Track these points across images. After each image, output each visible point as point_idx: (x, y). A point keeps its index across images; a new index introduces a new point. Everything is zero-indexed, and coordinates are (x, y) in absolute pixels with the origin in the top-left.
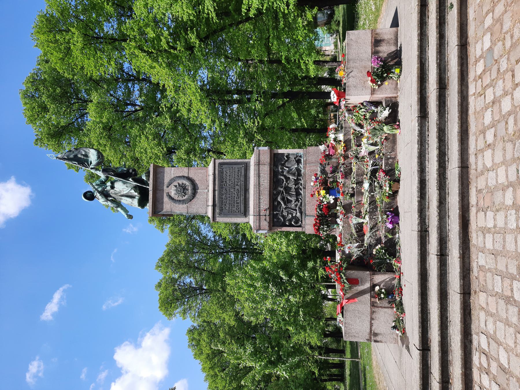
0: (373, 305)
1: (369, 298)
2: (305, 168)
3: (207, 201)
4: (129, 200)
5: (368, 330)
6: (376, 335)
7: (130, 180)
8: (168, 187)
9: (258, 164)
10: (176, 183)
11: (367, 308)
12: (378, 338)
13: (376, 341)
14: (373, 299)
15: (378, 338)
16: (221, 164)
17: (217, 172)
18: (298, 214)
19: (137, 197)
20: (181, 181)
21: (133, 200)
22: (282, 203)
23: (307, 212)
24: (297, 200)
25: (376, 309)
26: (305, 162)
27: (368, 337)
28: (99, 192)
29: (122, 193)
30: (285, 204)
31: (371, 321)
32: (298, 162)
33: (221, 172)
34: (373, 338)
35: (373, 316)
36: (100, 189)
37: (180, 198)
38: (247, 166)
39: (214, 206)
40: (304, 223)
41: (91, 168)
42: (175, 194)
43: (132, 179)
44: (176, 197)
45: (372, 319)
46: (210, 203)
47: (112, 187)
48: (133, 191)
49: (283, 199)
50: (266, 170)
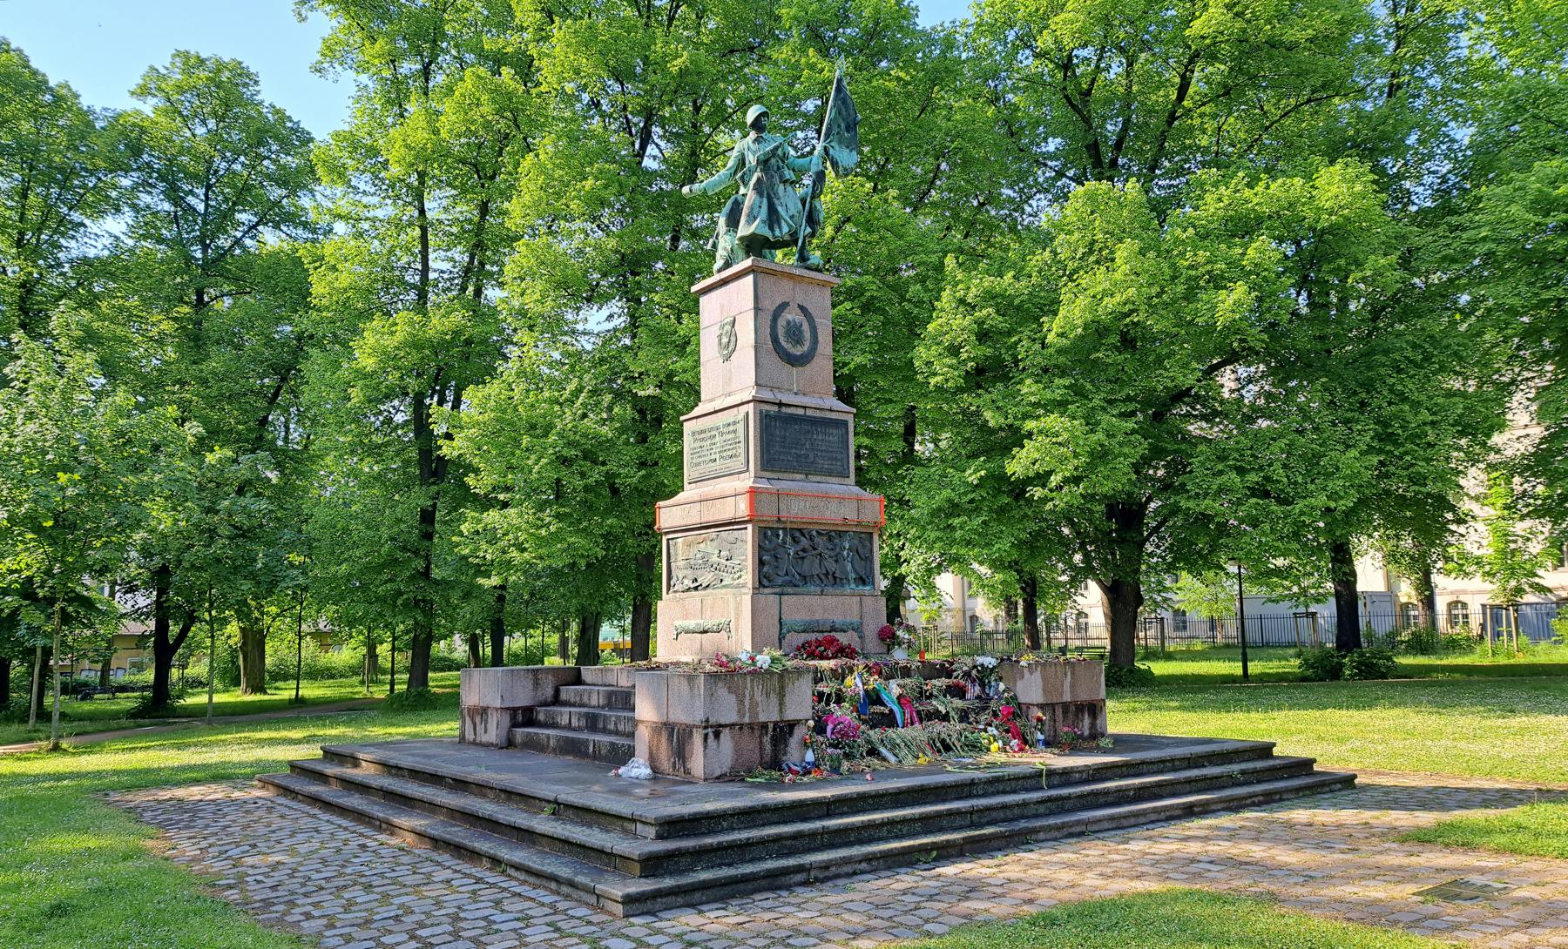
5: (723, 721)
6: (717, 735)
10: (806, 327)
16: (845, 423)
17: (833, 416)
18: (779, 581)
19: (768, 234)
20: (807, 335)
22: (800, 547)
23: (785, 598)
25: (757, 733)
27: (712, 721)
28: (776, 148)
35: (746, 730)
39: (780, 404)
42: (788, 322)
44: (781, 323)
48: (785, 229)
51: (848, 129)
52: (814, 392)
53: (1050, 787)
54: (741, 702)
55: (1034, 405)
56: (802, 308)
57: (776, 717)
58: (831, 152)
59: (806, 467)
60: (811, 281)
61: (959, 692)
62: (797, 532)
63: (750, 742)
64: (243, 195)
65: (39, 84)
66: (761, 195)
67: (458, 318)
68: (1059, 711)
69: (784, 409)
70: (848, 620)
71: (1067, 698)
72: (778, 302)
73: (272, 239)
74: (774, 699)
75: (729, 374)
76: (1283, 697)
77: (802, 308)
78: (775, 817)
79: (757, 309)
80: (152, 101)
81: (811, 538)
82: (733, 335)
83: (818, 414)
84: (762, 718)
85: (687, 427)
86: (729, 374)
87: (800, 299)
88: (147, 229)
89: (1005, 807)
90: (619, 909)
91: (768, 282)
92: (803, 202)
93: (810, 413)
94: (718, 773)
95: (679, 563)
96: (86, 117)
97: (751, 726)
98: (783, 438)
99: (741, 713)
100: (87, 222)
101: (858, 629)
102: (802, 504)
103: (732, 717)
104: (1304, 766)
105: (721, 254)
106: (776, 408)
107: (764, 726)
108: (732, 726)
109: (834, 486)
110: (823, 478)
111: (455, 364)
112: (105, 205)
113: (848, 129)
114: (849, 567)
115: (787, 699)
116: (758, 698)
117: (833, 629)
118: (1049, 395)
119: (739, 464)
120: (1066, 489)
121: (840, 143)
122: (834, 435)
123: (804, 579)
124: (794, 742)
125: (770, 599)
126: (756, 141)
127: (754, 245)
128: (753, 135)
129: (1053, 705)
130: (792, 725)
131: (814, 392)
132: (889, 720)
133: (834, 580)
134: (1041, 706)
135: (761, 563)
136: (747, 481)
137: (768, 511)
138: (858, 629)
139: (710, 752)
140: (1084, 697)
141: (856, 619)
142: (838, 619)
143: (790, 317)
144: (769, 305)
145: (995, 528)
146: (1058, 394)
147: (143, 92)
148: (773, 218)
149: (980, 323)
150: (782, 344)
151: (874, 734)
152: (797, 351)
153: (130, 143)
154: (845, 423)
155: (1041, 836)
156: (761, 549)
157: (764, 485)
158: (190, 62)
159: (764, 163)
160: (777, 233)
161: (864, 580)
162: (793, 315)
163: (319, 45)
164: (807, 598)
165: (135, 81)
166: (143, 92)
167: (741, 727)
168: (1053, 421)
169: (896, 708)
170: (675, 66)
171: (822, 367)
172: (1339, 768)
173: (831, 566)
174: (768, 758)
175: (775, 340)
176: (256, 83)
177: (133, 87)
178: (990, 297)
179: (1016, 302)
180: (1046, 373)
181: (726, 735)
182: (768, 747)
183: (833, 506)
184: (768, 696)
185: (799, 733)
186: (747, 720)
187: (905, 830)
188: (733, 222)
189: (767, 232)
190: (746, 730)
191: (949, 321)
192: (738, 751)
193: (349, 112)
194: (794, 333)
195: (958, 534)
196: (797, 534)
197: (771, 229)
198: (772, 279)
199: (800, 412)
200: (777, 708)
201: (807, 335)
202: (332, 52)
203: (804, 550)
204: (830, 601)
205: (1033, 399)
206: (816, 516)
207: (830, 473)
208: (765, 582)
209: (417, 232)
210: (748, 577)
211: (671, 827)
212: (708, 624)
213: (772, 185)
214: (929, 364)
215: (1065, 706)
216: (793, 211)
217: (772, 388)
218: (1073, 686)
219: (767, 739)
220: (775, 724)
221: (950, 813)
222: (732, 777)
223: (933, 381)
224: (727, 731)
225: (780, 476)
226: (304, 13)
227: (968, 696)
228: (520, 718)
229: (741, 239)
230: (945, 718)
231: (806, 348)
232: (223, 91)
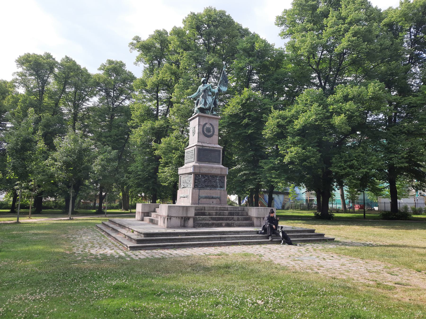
0: (182, 218)
2: (219, 190)
3: (204, 143)
4: (203, 103)
5: (172, 216)
6: (170, 219)
9: (221, 168)
10: (211, 128)
11: (181, 215)
12: (169, 219)
13: (168, 219)
16: (220, 151)
17: (217, 149)
18: (200, 186)
19: (204, 107)
20: (212, 130)
23: (200, 190)
24: (206, 186)
26: (221, 190)
33: (217, 150)
35: (177, 218)
36: (208, 88)
37: (205, 130)
38: (219, 163)
39: (203, 146)
44: (205, 127)
45: (176, 217)
46: (204, 145)
47: (209, 95)
48: (208, 106)
49: (206, 180)
50: (218, 172)
51: (225, 82)
52: (214, 143)
53: (194, 227)
56: (211, 124)
57: (185, 216)
58: (220, 88)
64: (122, 92)
65: (79, 68)
67: (162, 122)
68: (262, 219)
73: (127, 103)
75: (193, 140)
76: (403, 227)
77: (211, 124)
79: (199, 125)
81: (209, 177)
82: (195, 130)
83: (213, 148)
85: (186, 151)
86: (193, 140)
87: (210, 122)
88: (101, 101)
90: (129, 249)
91: (202, 119)
92: (213, 100)
93: (210, 148)
95: (182, 182)
96: (89, 76)
98: (203, 154)
104: (322, 235)
105: (195, 111)
109: (216, 166)
111: (159, 134)
112: (92, 94)
113: (225, 82)
119: (193, 160)
123: (207, 186)
126: (203, 86)
127: (201, 110)
128: (202, 85)
129: (260, 218)
131: (214, 143)
133: (215, 187)
135: (195, 182)
136: (194, 164)
143: (207, 126)
144: (202, 123)
147: (100, 69)
148: (205, 103)
150: (205, 132)
152: (209, 134)
154: (220, 151)
156: (195, 179)
157: (197, 164)
158: (110, 62)
159: (204, 91)
161: (222, 187)
162: (208, 126)
163: (136, 58)
165: (99, 66)
166: (100, 69)
170: (210, 62)
171: (216, 138)
172: (331, 237)
174: (182, 224)
175: (203, 131)
183: (214, 170)
188: (197, 105)
189: (203, 107)
190: (177, 218)
194: (208, 130)
197: (205, 106)
199: (208, 148)
201: (212, 130)
202: (139, 60)
209: (156, 101)
210: (192, 186)
211: (147, 235)
212: (185, 196)
213: (206, 96)
217: (202, 143)
220: (185, 217)
228: (146, 214)
229: (198, 108)
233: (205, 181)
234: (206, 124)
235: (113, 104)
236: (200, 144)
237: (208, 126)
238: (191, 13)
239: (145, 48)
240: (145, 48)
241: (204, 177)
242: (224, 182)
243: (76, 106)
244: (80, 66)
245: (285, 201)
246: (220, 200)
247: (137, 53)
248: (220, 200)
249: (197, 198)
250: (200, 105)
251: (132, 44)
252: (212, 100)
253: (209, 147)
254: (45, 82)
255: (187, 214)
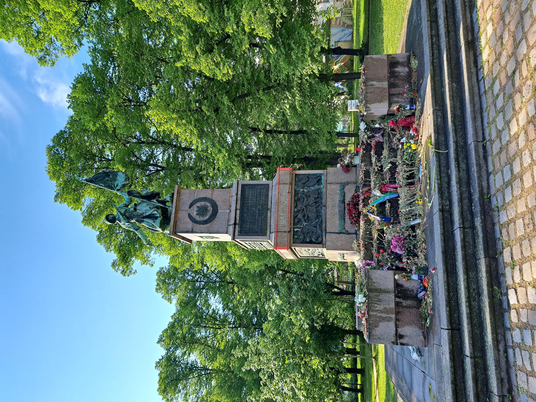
1: (393, 297)
4: (150, 221)
5: (394, 332)
6: (401, 337)
7: (155, 201)
8: (190, 208)
10: (199, 204)
12: (404, 341)
14: (397, 300)
15: (404, 341)
17: (239, 193)
18: (319, 231)
19: (159, 219)
21: (154, 222)
22: (303, 220)
23: (328, 230)
25: (401, 310)
27: (393, 339)
29: (144, 215)
30: (305, 221)
31: (396, 323)
32: (319, 182)
34: (398, 341)
35: (399, 317)
36: (123, 211)
39: (235, 224)
40: (324, 240)
41: (118, 190)
42: (197, 214)
43: (157, 200)
44: (198, 218)
46: (232, 222)
50: (286, 189)
54: (384, 319)
55: (238, 27)
56: (191, 206)
57: (392, 296)
58: (118, 188)
59: (264, 209)
60: (178, 201)
61: (379, 147)
62: (295, 220)
63: (408, 315)
66: (143, 221)
68: (394, 91)
69: (237, 222)
70: (338, 192)
71: (385, 84)
72: (188, 220)
74: (383, 296)
77: (191, 206)
78: (459, 372)
80: (172, 297)
81: (298, 211)
83: (239, 202)
84: (393, 305)
89: (461, 200)
91: (181, 226)
93: (238, 207)
94: (422, 338)
97: (397, 313)
99: (389, 320)
100: (212, 308)
101: (343, 185)
102: (282, 218)
103: (392, 325)
106: (237, 226)
107: (397, 304)
108: (397, 326)
109: (273, 193)
110: (270, 199)
114: (312, 188)
115: (383, 287)
116: (380, 307)
117: (343, 202)
118: (232, 19)
120: (277, 6)
121: (115, 180)
122: (249, 193)
123: (318, 216)
124: (407, 285)
125: (329, 238)
129: (391, 95)
130: (397, 285)
132: (394, 202)
134: (390, 105)
135: (311, 242)
137: (285, 238)
138: (343, 185)
139: (411, 342)
140: (385, 71)
141: (338, 187)
142: (338, 198)
143: (195, 213)
144: (190, 225)
145: (296, 36)
146: (232, 15)
147: (170, 300)
148: (152, 217)
149: (204, 52)
151: (403, 223)
152: (210, 209)
153: (186, 304)
155: (485, 184)
159: (128, 219)
160: (158, 215)
161: (318, 180)
164: (328, 217)
167: (397, 320)
168: (244, 20)
169: (387, 197)
173: (312, 200)
175: (205, 222)
176: (163, 268)
177: (169, 303)
178: (191, 47)
179: (192, 35)
180: (223, 20)
181: (401, 331)
182: (409, 302)
183: (283, 199)
184: (380, 301)
185: (403, 281)
186: (393, 316)
187: (474, 286)
190: (399, 317)
191: (204, 65)
192: (410, 324)
193: (164, 255)
194: (202, 211)
195: (299, 55)
196: (296, 220)
197: (156, 218)
198: (178, 223)
199: (238, 212)
200: (387, 295)
201: (203, 203)
202: (145, 261)
203: (304, 216)
204: (329, 203)
205: (235, 27)
206: (287, 210)
207: (267, 196)
208: (320, 239)
213: (138, 216)
214: (224, 75)
215: (391, 85)
216: (148, 208)
218: (379, 80)
219: (405, 303)
220: (396, 296)
221: (464, 247)
222: (427, 334)
223: (231, 74)
224: (399, 330)
225: (269, 225)
226: (133, 271)
227: (381, 140)
230: (394, 166)
231: (209, 205)
232: (167, 279)
233: (308, 219)
234: (190, 216)
235: (215, 281)
236: (231, 228)
237: (194, 214)
238: (56, 201)
239: (125, 257)
240: (125, 257)
241: (300, 220)
242: (308, 176)
243: (224, 321)
244: (170, 323)
245: (340, 24)
246: (348, 183)
247: (136, 263)
248: (348, 183)
249: (344, 236)
250: (156, 228)
251: (123, 272)
252: (145, 204)
253: (236, 210)
254: (192, 368)
255: (387, 292)
